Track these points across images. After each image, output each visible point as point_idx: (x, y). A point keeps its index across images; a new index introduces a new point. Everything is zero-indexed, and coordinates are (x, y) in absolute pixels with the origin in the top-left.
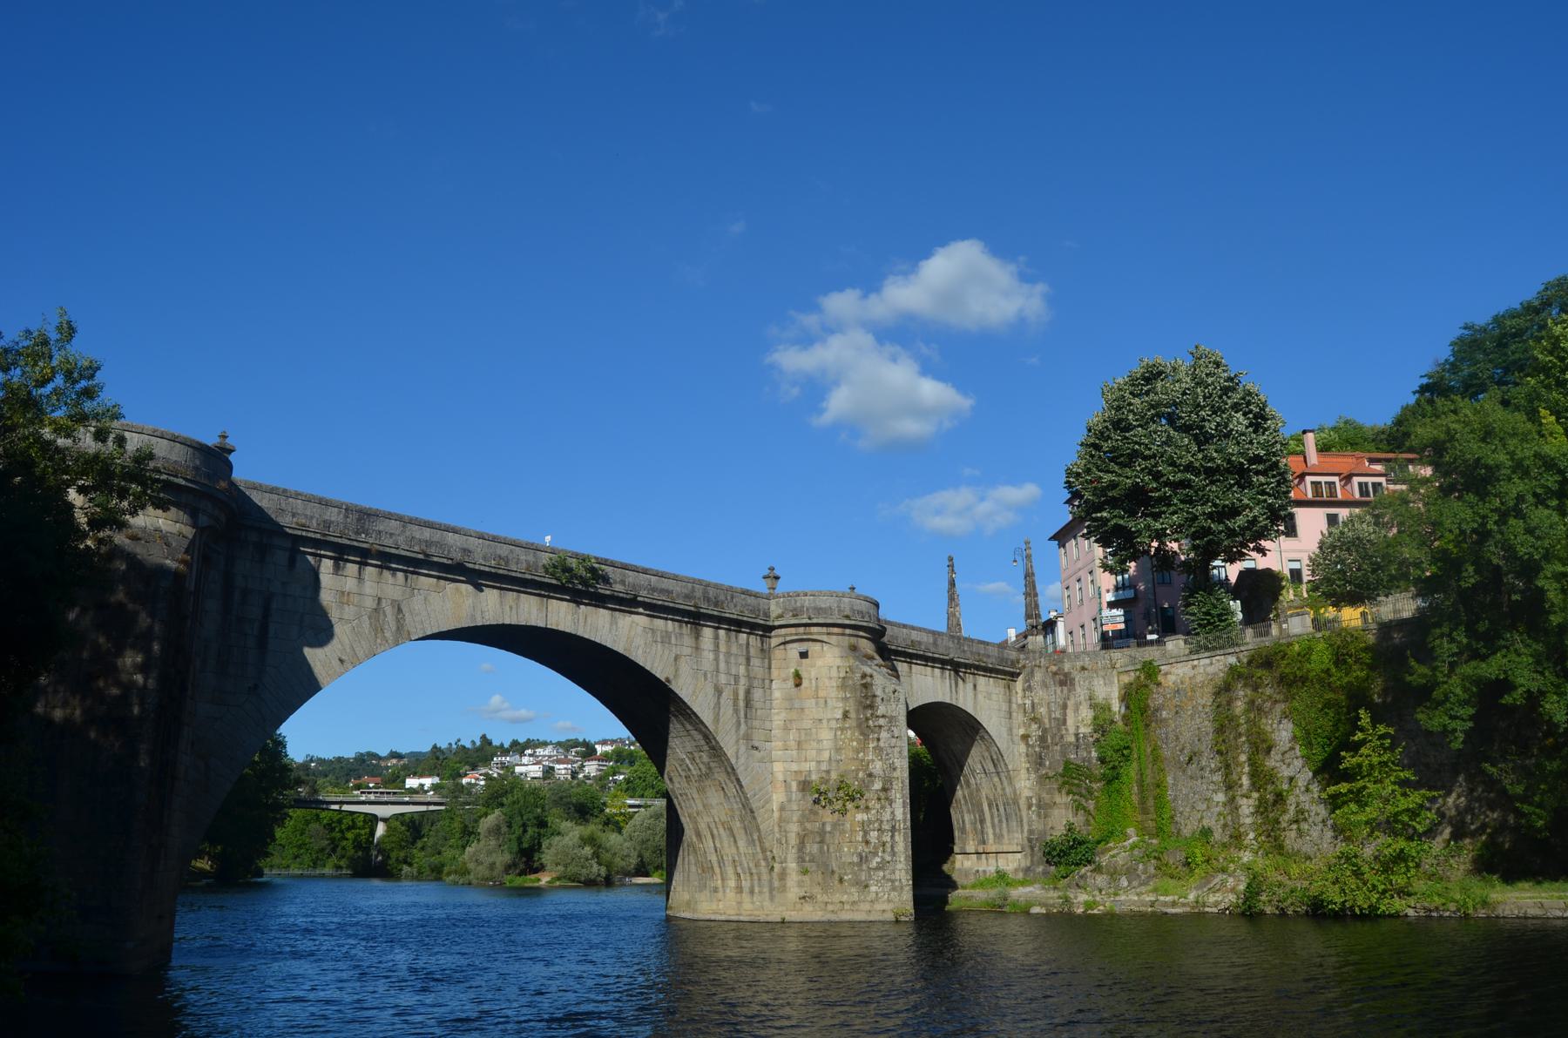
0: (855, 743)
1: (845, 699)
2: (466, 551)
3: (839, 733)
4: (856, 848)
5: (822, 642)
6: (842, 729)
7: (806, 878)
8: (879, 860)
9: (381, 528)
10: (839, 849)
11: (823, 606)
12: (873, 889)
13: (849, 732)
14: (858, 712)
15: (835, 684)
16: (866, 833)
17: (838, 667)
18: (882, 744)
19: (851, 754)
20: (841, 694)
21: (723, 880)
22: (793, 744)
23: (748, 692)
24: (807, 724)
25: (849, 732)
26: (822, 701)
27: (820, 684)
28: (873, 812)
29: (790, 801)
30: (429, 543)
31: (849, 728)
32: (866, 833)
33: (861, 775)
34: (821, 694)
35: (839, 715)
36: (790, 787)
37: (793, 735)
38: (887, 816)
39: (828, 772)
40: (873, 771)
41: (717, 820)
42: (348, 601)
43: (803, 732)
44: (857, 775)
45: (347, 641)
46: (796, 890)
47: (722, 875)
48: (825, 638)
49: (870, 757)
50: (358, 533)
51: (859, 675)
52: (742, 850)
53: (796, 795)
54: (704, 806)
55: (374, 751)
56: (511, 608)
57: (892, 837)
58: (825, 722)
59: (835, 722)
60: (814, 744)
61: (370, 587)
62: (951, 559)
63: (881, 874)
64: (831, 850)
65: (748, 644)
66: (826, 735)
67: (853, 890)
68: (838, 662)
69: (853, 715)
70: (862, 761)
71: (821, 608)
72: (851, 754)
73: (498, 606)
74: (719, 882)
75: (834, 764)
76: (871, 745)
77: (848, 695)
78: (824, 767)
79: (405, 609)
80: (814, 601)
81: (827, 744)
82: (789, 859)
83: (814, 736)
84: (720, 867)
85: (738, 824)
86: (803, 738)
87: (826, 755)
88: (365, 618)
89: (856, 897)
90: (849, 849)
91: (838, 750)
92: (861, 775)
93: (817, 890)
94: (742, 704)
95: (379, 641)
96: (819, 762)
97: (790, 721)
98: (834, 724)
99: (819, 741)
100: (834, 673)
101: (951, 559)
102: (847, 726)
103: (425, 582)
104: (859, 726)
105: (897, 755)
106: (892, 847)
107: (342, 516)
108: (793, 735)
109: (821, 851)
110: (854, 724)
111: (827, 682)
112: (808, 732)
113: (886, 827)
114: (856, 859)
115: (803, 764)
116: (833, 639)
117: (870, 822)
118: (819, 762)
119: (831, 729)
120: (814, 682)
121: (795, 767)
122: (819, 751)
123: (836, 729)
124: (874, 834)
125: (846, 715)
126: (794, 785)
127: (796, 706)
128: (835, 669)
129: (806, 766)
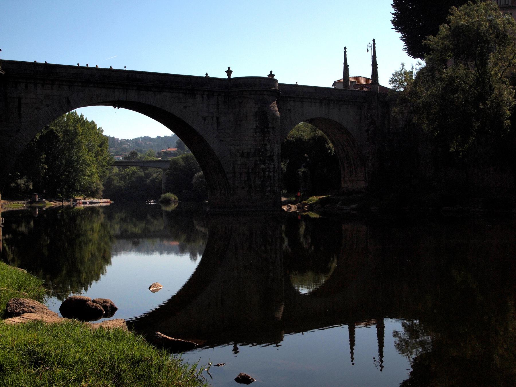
3: (254, 134)
5: (247, 98)
6: (256, 132)
8: (268, 183)
12: (267, 194)
13: (258, 134)
16: (264, 173)
17: (254, 108)
18: (270, 138)
28: (267, 164)
35: (254, 127)
38: (271, 166)
39: (251, 149)
40: (267, 149)
55: (146, 135)
57: (274, 174)
62: (345, 48)
63: (269, 188)
65: (218, 98)
76: (266, 139)
77: (258, 119)
101: (345, 48)
105: (276, 142)
106: (274, 178)
113: (271, 170)
120: (245, 114)
124: (267, 173)
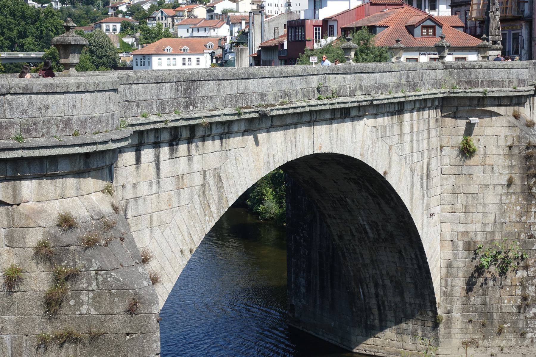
0: (518, 208)
1: (511, 166)
2: (263, 95)
3: (504, 197)
4: (516, 301)
6: (507, 194)
7: (470, 326)
9: (203, 93)
10: (500, 300)
11: (496, 78)
12: (529, 335)
14: (522, 179)
15: (502, 153)
16: (524, 287)
17: (506, 136)
19: (514, 218)
20: (508, 162)
21: (381, 321)
22: (460, 207)
23: (428, 164)
24: (474, 189)
25: (514, 197)
26: (489, 168)
27: (488, 152)
28: (532, 269)
29: (456, 259)
30: (236, 98)
31: (514, 194)
32: (524, 287)
33: (523, 236)
34: (489, 161)
36: (457, 247)
37: (461, 198)
39: (493, 233)
41: (384, 273)
42: (183, 184)
43: (470, 196)
44: (519, 236)
45: (185, 229)
46: (459, 336)
47: (380, 314)
48: (495, 109)
49: (532, 221)
50: (187, 107)
51: (524, 145)
52: (407, 300)
53: (462, 253)
54: (372, 261)
56: (291, 143)
58: (491, 187)
59: (500, 188)
60: (480, 208)
61: (197, 165)
64: (493, 302)
66: (492, 199)
67: (511, 336)
68: (506, 131)
69: (517, 181)
70: (525, 223)
71: (494, 81)
72: (514, 218)
73: (283, 144)
74: (377, 322)
75: (498, 226)
77: (514, 163)
78: (489, 229)
79: (223, 176)
80: (489, 73)
81: (493, 208)
82: (454, 310)
83: (480, 200)
84: (379, 309)
85: (408, 280)
86: (470, 202)
87: (491, 218)
88: (196, 197)
89: (513, 343)
90: (509, 301)
91: (503, 213)
92: (523, 236)
93: (477, 336)
94: (425, 178)
95: (207, 218)
96: (484, 224)
97: (459, 186)
98: (499, 190)
99: (485, 205)
100: (502, 142)
102: (512, 191)
103: (235, 141)
104: (523, 191)
107: (173, 90)
108: (461, 198)
109: (484, 303)
110: (518, 190)
111: (494, 151)
112: (475, 196)
114: (514, 310)
115: (469, 225)
116: (501, 110)
117: (528, 278)
118: (484, 224)
119: (497, 194)
121: (461, 228)
122: (484, 214)
123: (501, 195)
125: (510, 182)
126: (461, 244)
127: (464, 172)
128: (502, 137)
129: (472, 228)
